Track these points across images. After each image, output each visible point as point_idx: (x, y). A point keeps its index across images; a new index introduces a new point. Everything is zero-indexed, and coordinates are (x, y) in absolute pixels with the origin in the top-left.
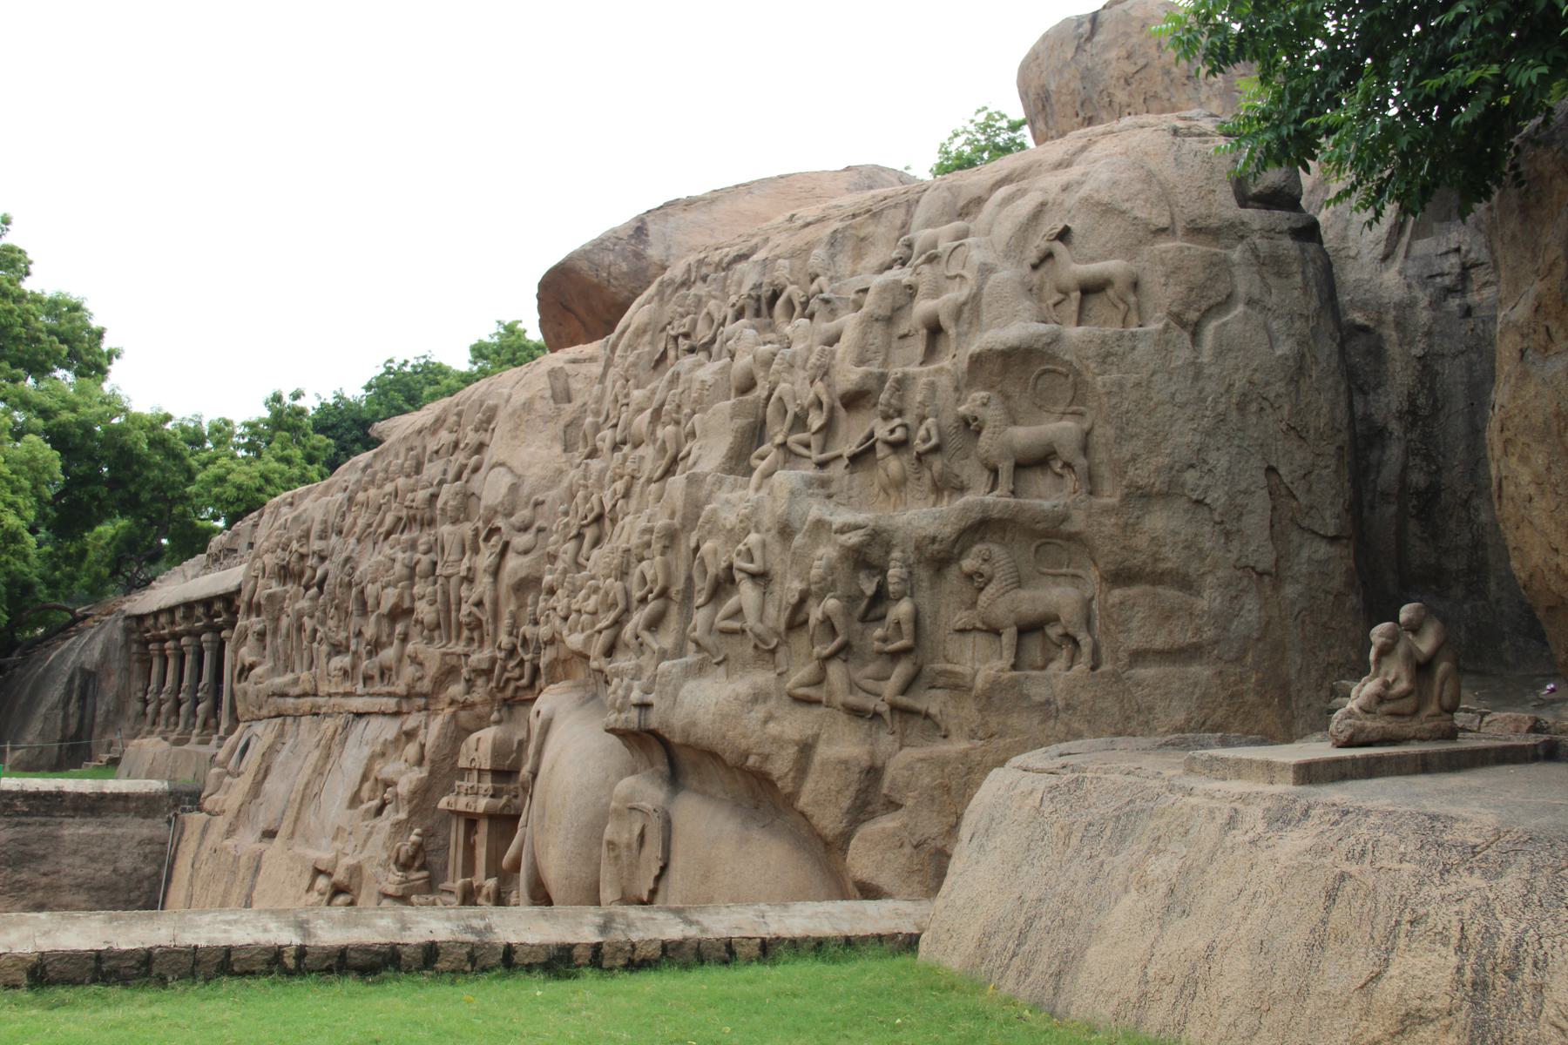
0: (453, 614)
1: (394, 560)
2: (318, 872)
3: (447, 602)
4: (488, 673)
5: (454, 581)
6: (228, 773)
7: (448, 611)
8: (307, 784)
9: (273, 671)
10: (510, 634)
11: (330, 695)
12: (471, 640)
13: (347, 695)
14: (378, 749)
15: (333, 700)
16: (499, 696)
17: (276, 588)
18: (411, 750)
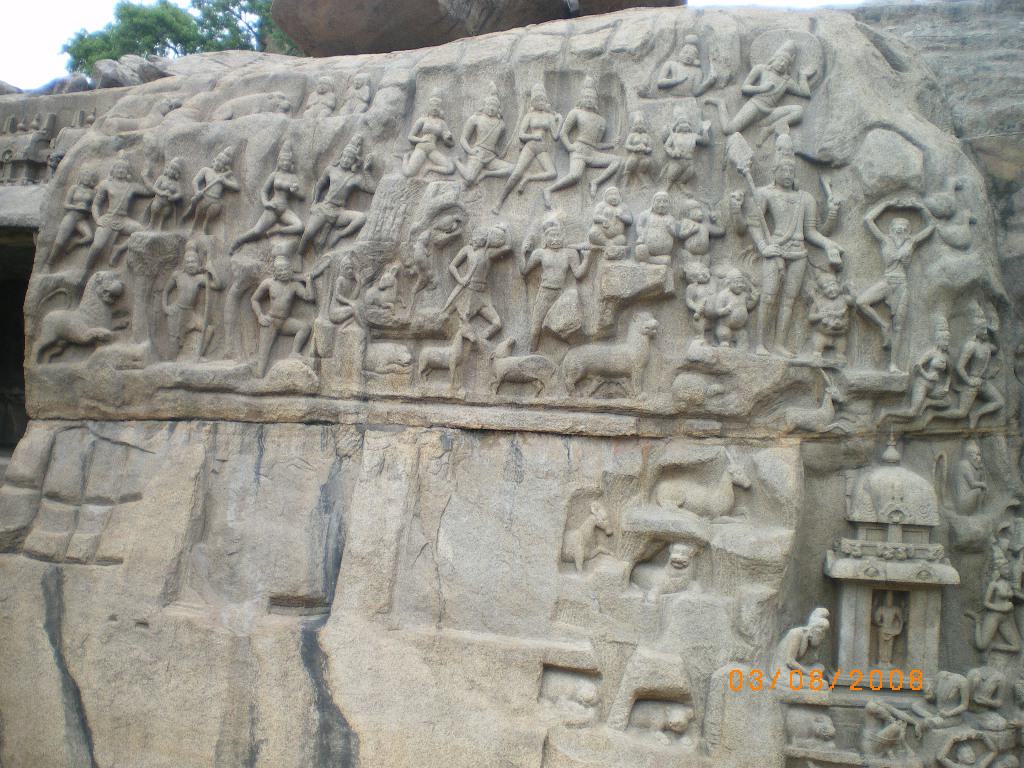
0: (785, 312)
1: (628, 225)
2: (549, 668)
3: (779, 293)
4: (879, 396)
5: (797, 268)
6: (54, 496)
7: (776, 305)
8: (400, 532)
9: (157, 353)
10: (945, 351)
11: (365, 399)
12: (828, 349)
13: (424, 400)
14: (593, 485)
15: (382, 407)
16: (899, 428)
17: (142, 232)
18: (718, 495)
